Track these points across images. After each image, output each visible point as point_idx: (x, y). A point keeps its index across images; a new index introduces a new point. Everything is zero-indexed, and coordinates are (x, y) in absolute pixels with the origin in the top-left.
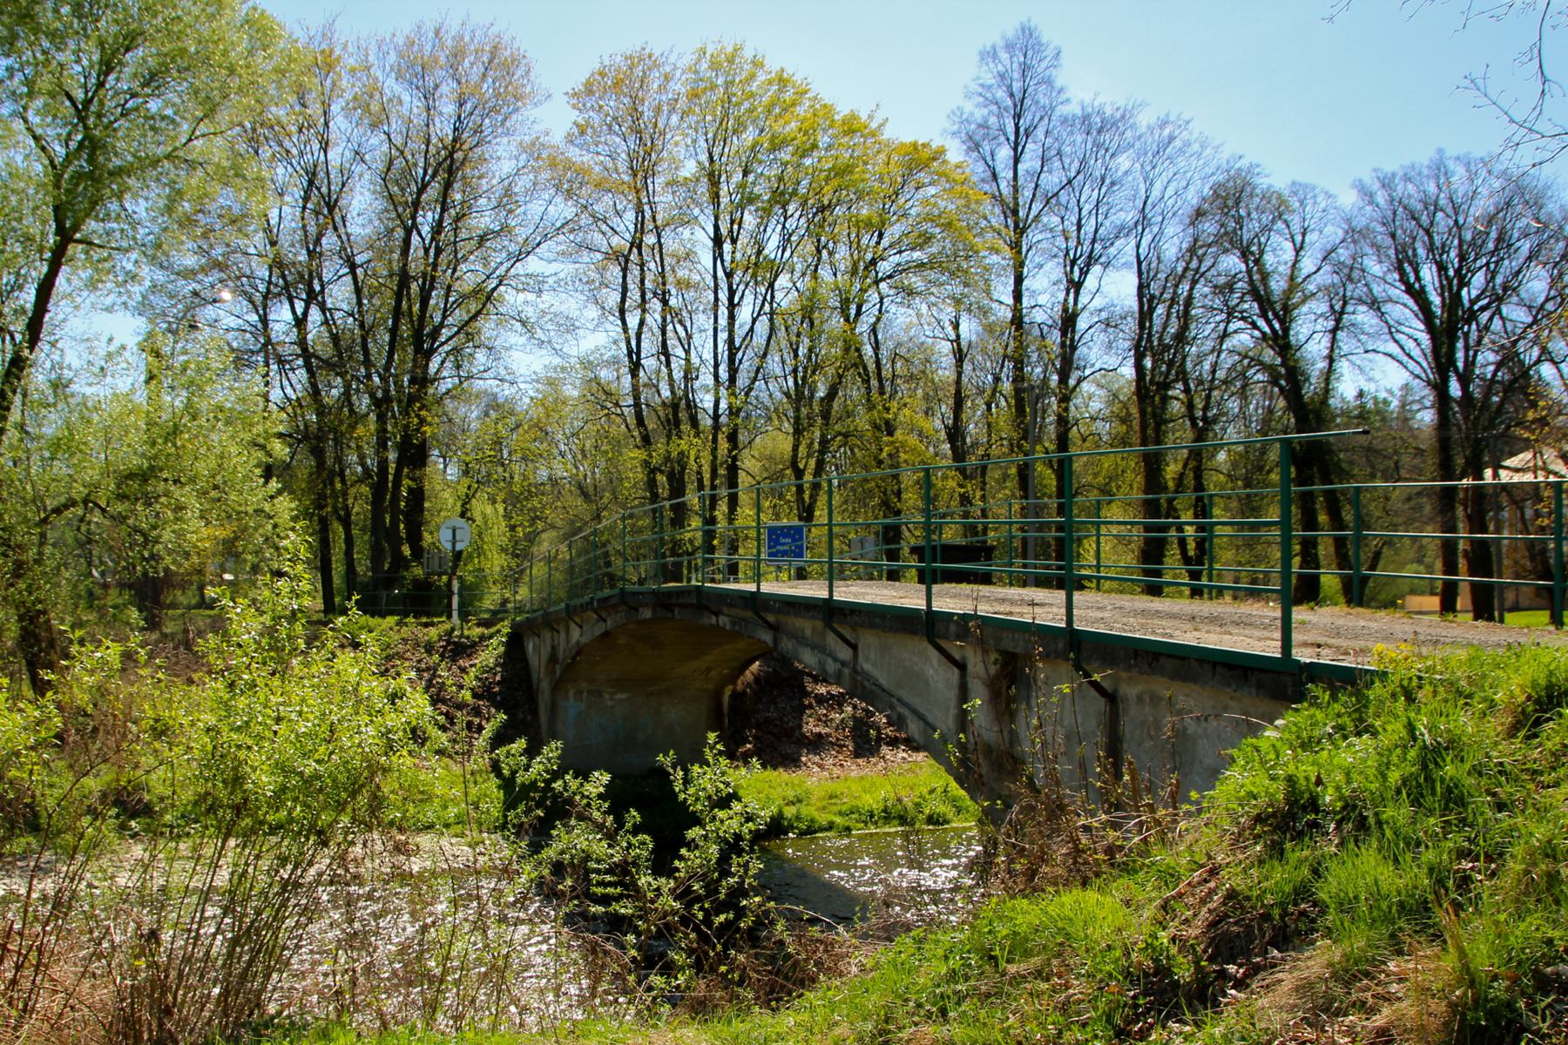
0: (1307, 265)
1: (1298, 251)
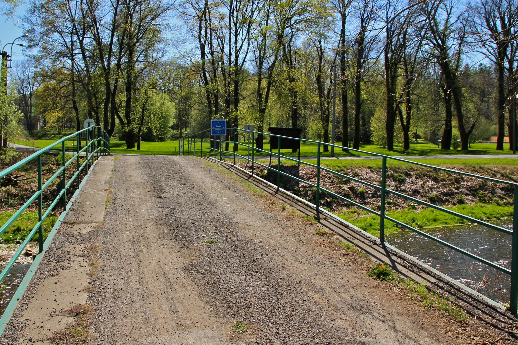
0: (452, 20)
1: (448, 15)
